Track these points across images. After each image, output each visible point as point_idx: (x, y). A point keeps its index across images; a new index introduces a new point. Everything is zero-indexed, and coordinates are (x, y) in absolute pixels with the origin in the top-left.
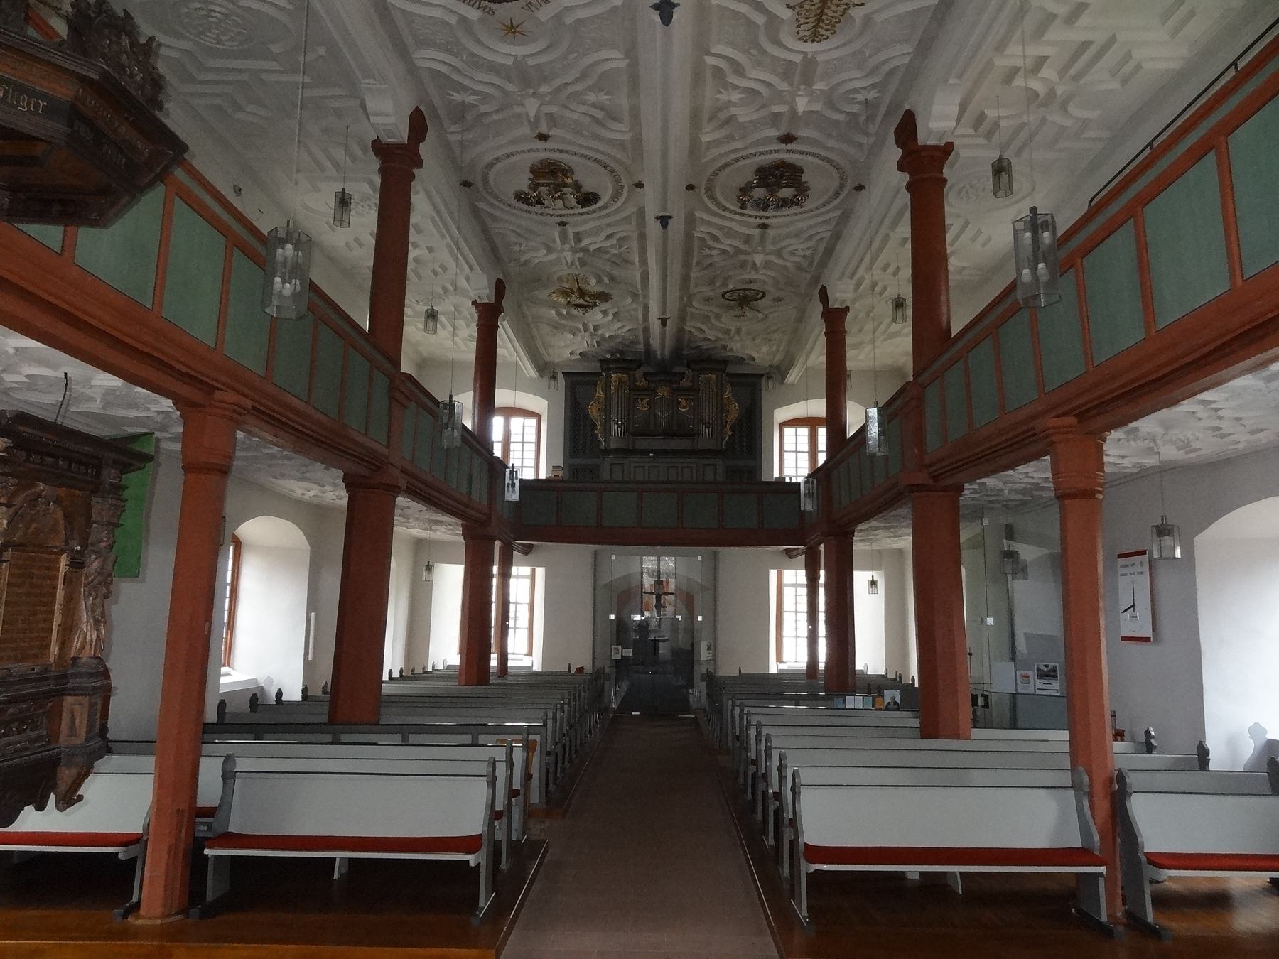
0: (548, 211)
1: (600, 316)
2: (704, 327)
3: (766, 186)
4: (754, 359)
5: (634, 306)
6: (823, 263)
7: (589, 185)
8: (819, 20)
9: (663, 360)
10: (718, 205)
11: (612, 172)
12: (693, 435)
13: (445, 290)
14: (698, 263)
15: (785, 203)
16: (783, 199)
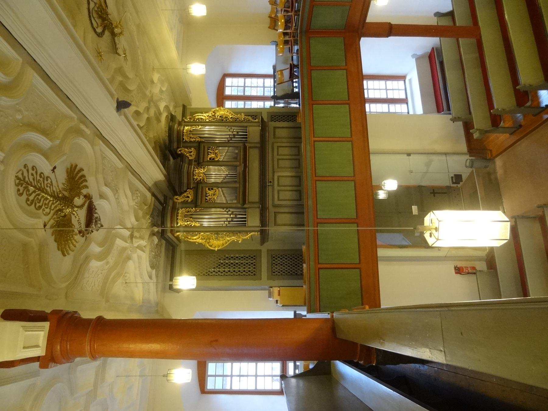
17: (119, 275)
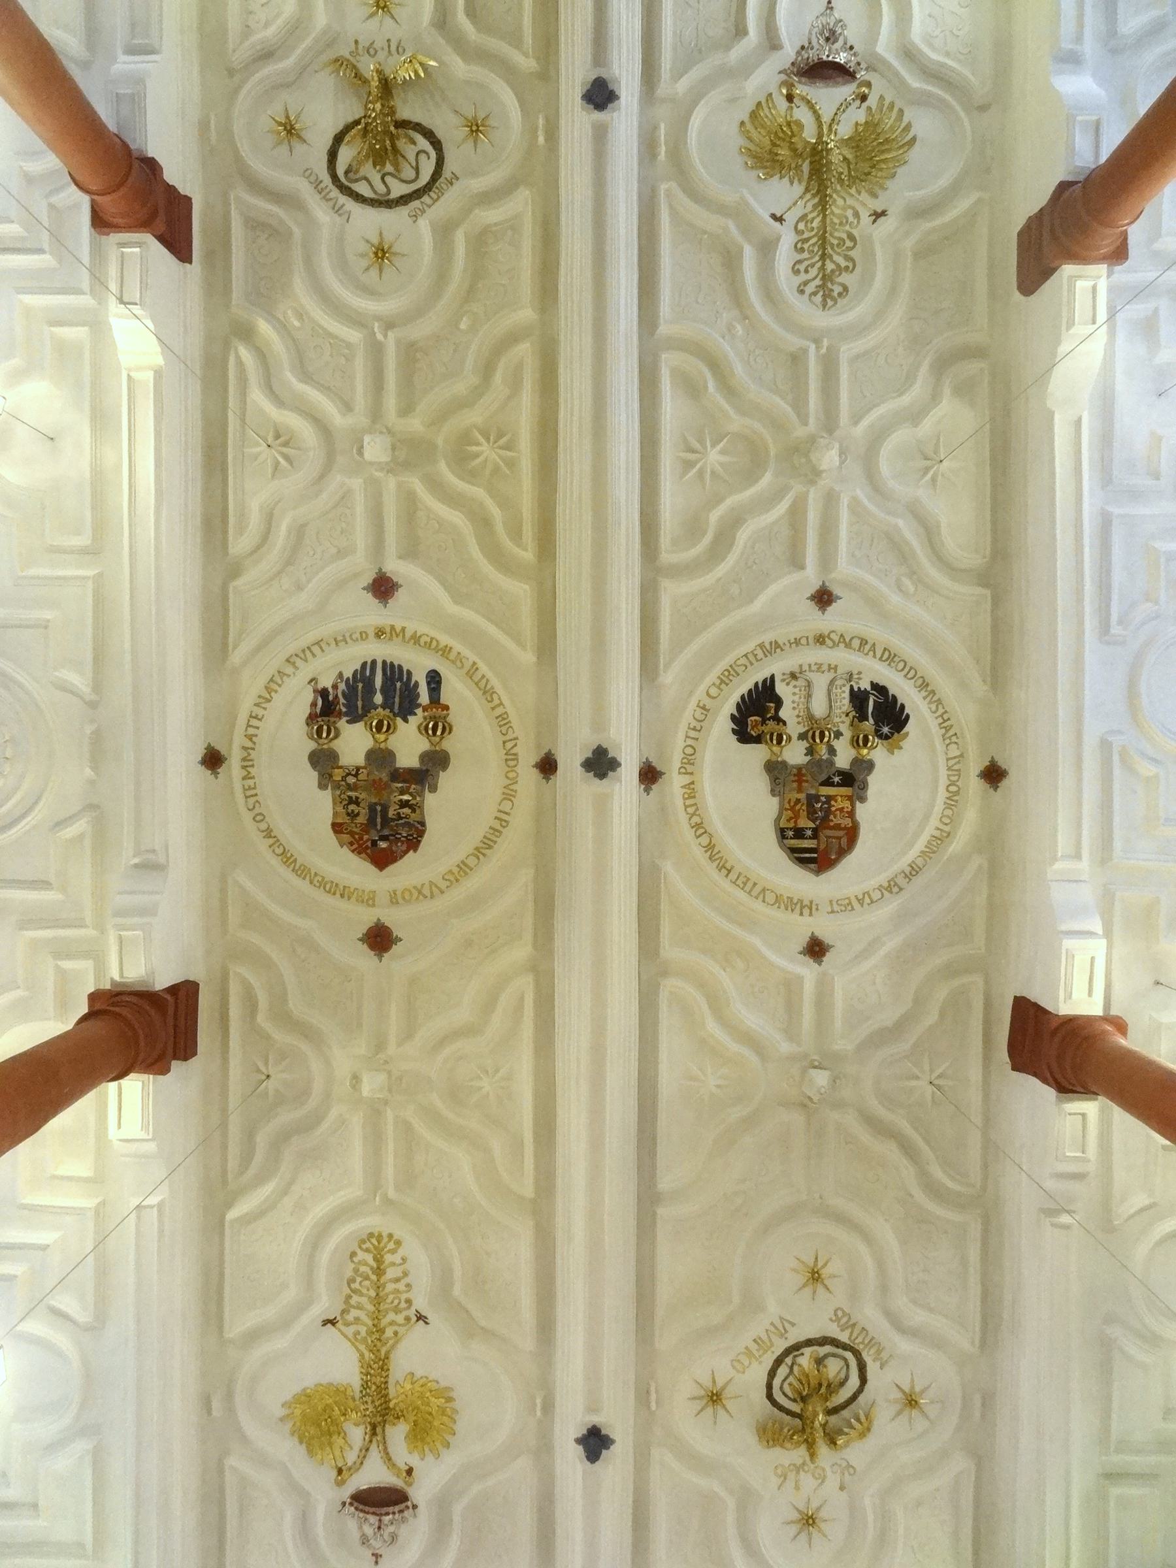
3: (398, 775)
8: (379, 1287)
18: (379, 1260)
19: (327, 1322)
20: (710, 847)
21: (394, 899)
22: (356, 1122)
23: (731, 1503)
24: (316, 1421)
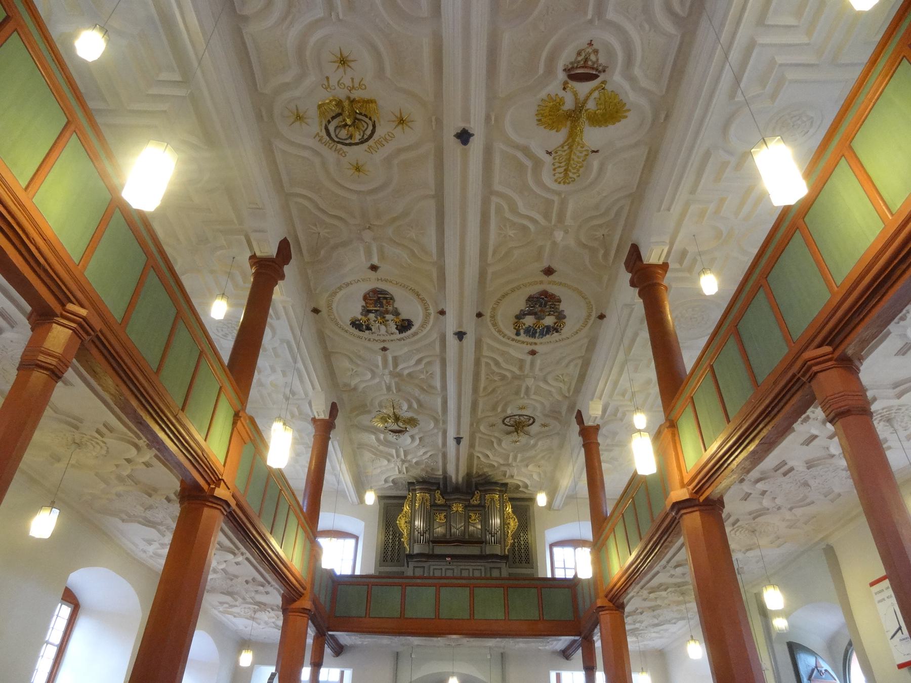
0: (372, 337)
1: (409, 440)
2: (489, 453)
3: (535, 314)
4: (526, 486)
5: (436, 431)
6: (577, 391)
7: (404, 316)
8: (568, 164)
9: (457, 483)
10: (499, 331)
11: (422, 300)
12: (482, 542)
13: (293, 416)
14: (485, 388)
15: (548, 330)
16: (548, 327)
17: (375, 454)
18: (566, 175)
19: (597, 151)
20: (418, 295)
21: (541, 282)
22: (569, 221)
23: (388, 72)
24: (611, 112)
